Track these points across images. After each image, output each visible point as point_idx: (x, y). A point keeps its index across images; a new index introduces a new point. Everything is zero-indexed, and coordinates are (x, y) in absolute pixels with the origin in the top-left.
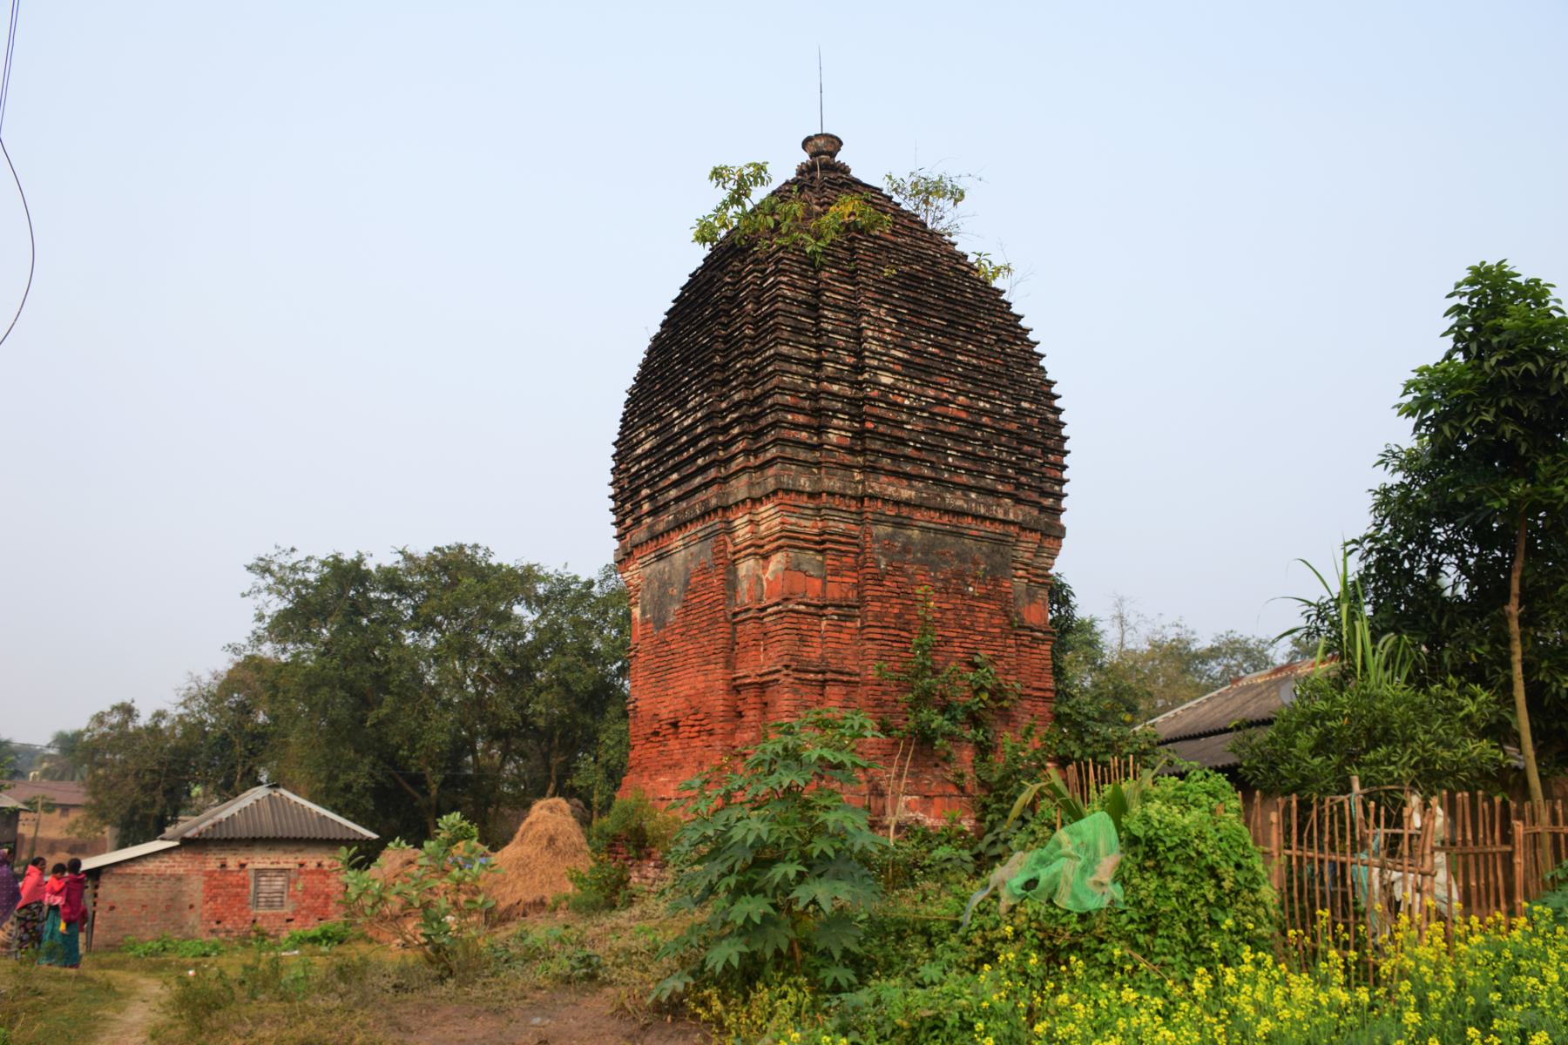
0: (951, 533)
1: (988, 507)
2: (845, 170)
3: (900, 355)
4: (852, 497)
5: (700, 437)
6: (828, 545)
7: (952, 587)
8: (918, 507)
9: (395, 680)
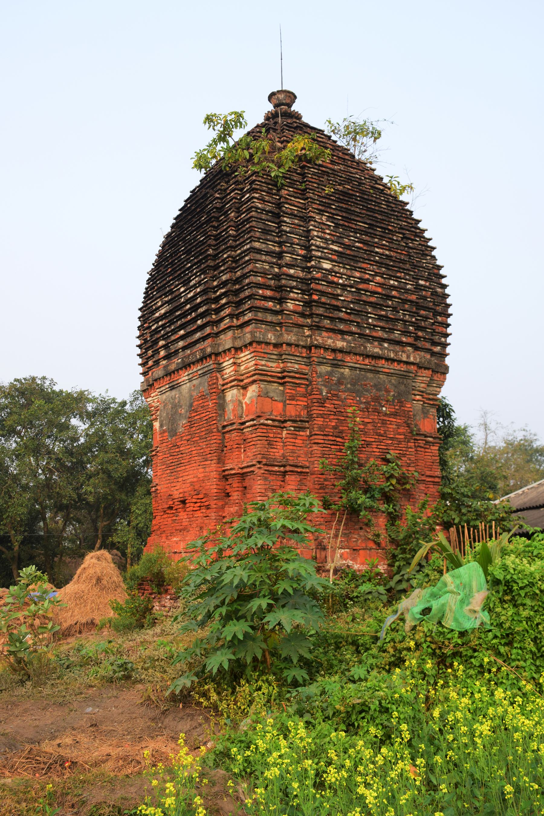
1: (396, 353)
2: (298, 116)
4: (303, 347)
5: (199, 306)
6: (287, 379)
7: (372, 407)
8: (349, 353)
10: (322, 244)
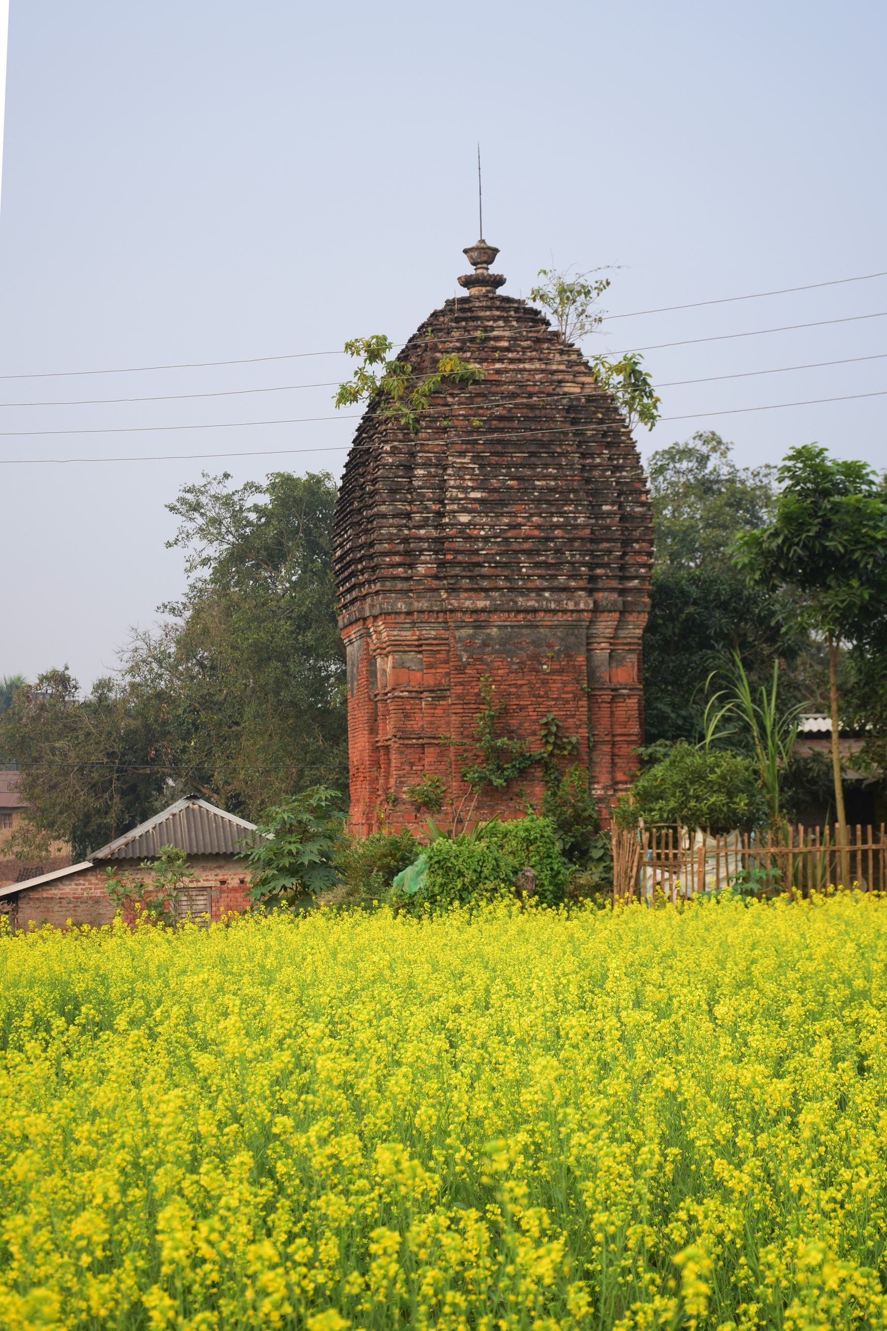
1: (558, 602)
3: (478, 495)
4: (438, 612)
6: (424, 648)
10: (461, 496)
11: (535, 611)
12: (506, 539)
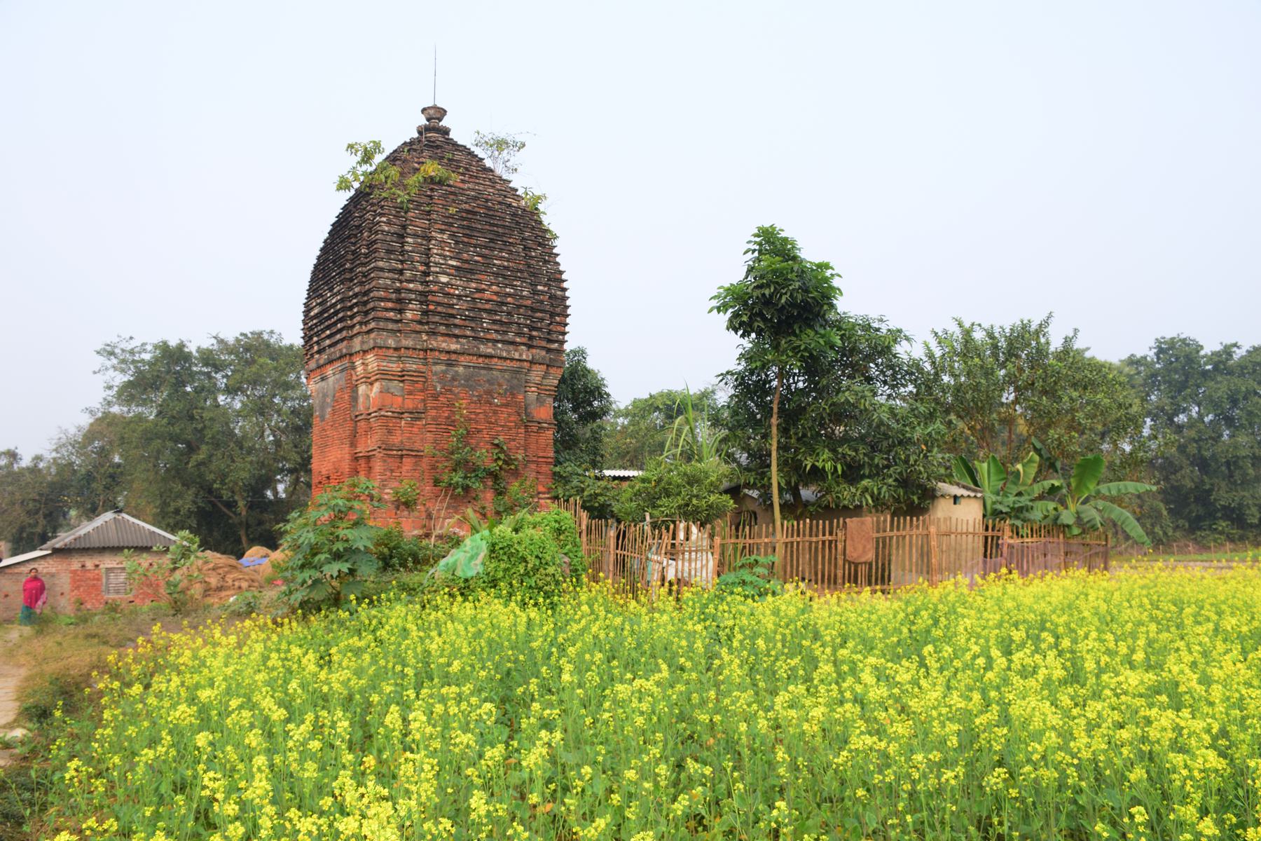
0: (484, 368)
1: (509, 352)
2: (446, 132)
3: (454, 263)
5: (336, 313)
9: (209, 434)
11: (491, 357)
12: (474, 299)
